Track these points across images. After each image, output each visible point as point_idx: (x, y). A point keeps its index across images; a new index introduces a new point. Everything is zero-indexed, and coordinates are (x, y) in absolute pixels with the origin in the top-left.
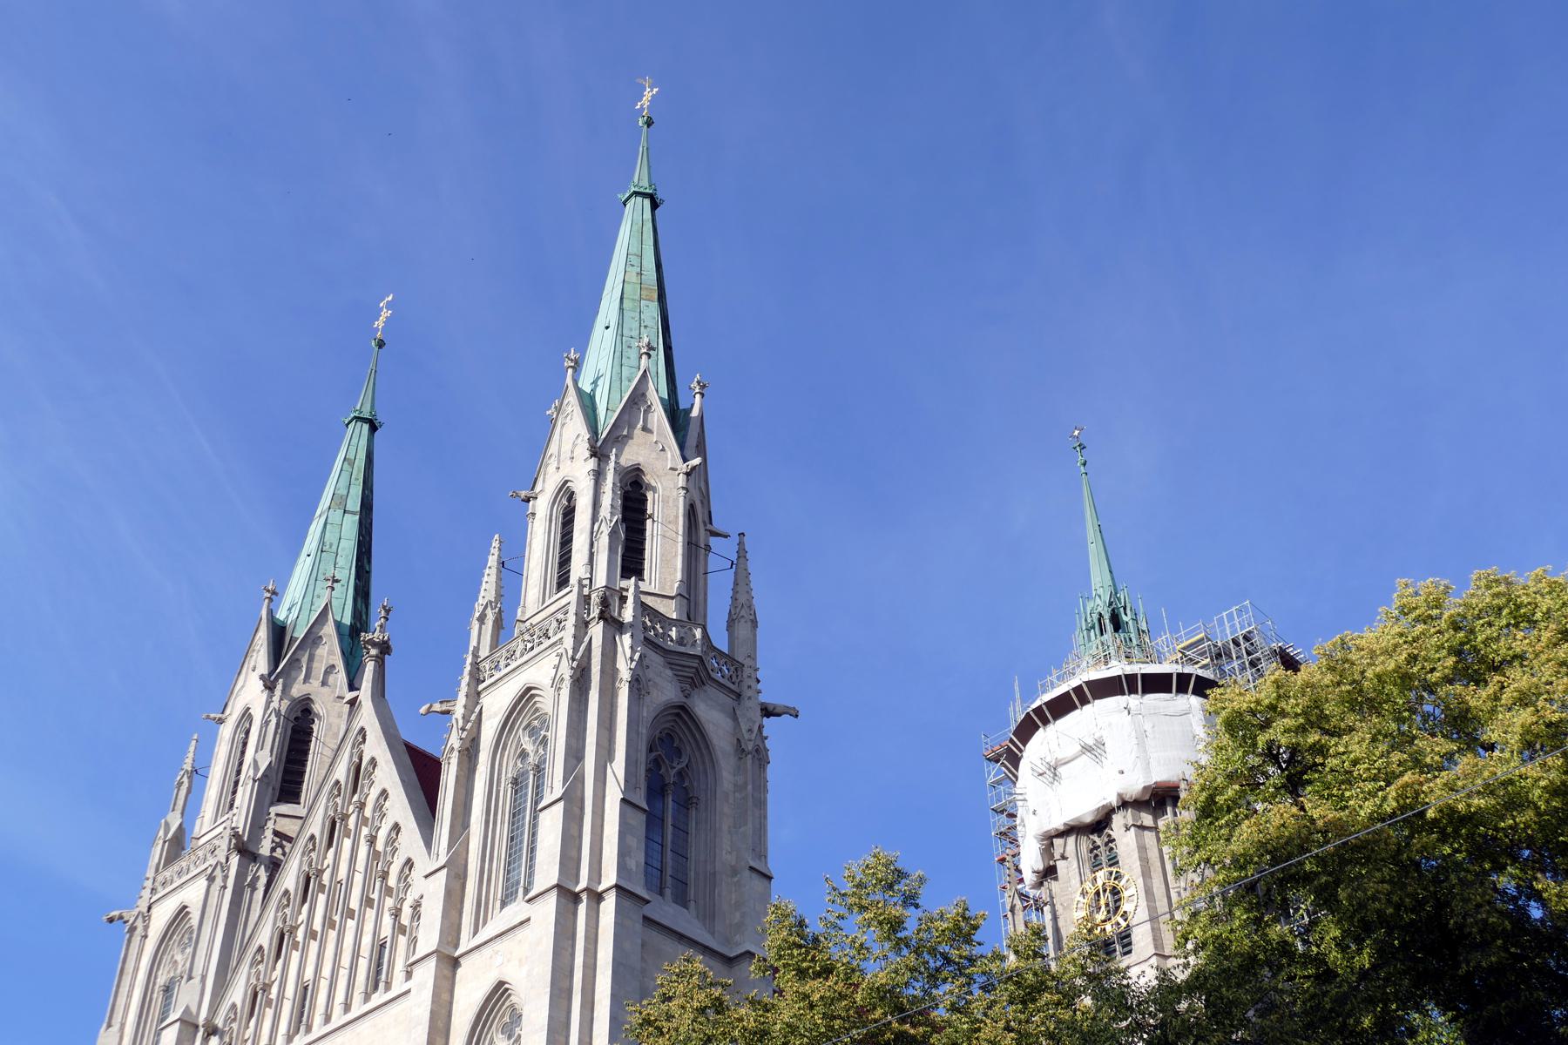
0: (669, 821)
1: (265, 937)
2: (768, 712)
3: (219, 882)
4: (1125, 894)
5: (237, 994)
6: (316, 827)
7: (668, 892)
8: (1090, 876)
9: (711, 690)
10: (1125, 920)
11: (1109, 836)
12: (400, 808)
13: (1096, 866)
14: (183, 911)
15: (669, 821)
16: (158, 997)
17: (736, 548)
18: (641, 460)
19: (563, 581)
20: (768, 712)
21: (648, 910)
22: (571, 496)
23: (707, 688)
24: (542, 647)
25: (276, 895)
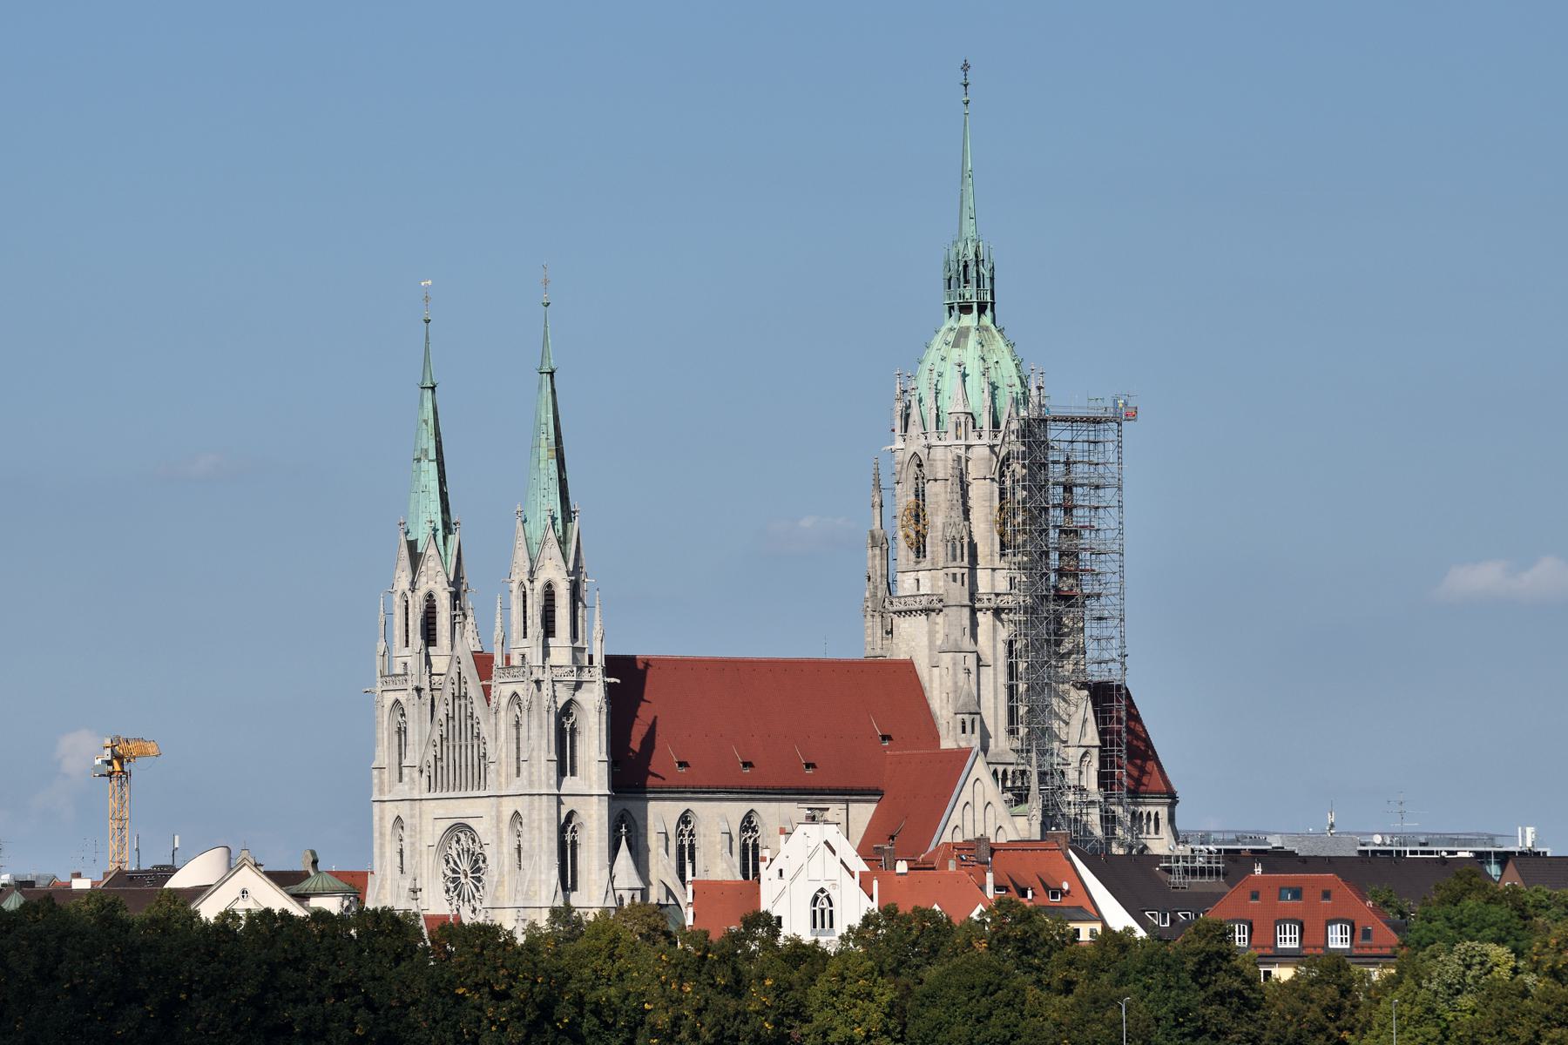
18: (550, 576)
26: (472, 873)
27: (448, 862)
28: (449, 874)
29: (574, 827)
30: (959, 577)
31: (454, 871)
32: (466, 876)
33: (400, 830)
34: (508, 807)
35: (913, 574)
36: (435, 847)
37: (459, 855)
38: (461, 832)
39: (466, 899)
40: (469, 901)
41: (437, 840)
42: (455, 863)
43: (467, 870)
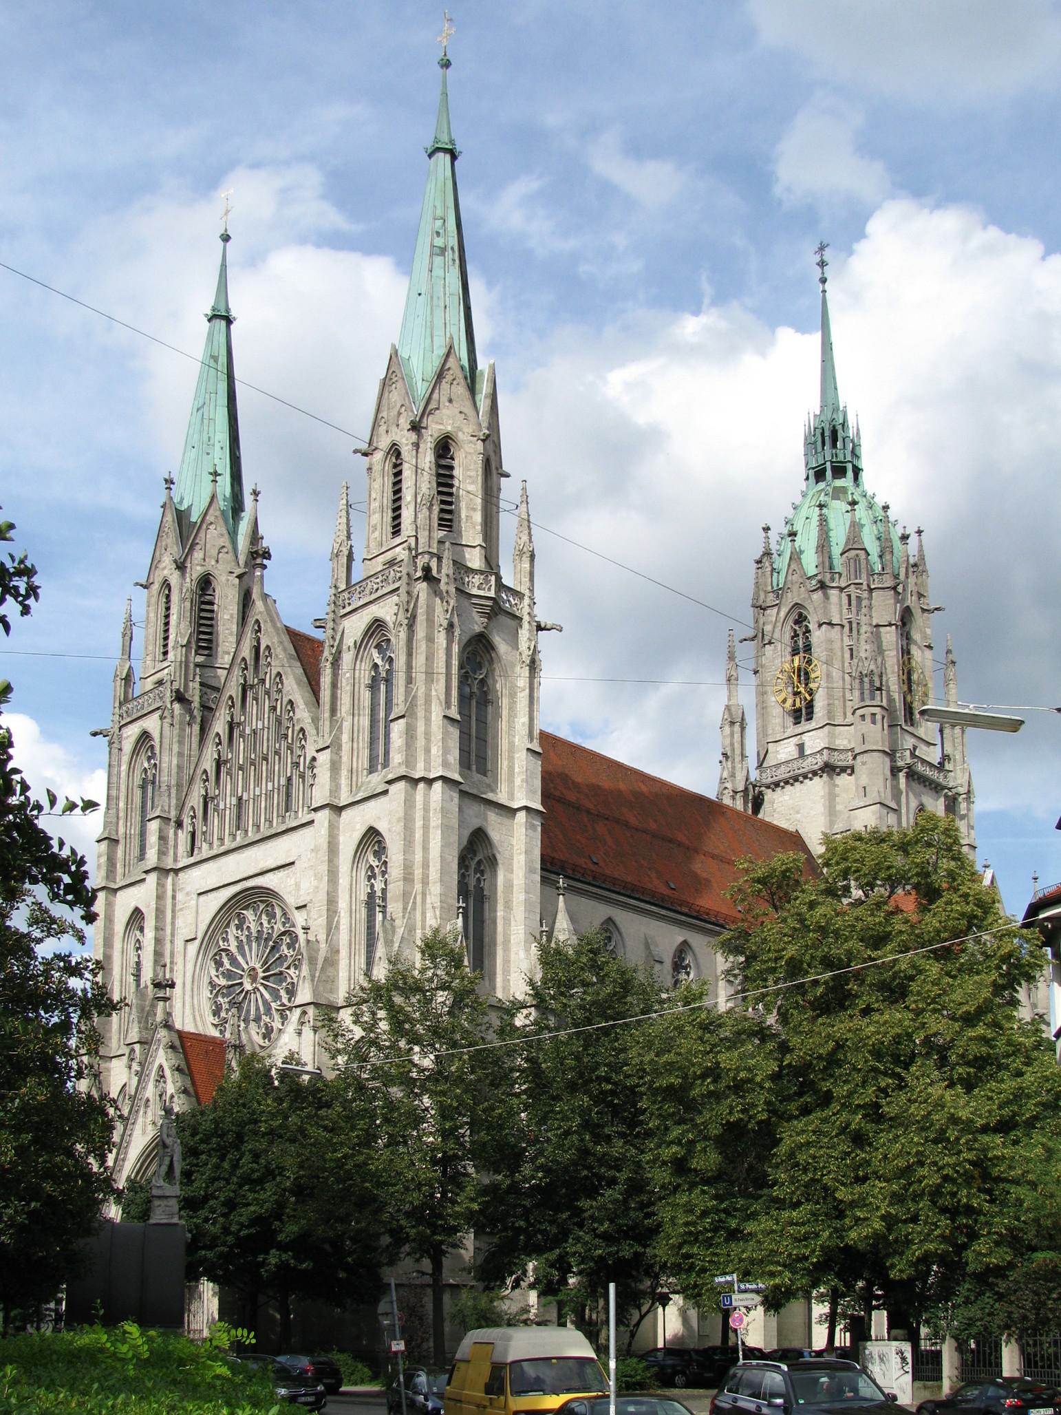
0: (474, 718)
1: (208, 764)
2: (540, 628)
3: (168, 720)
4: (813, 676)
5: (195, 800)
6: (233, 690)
7: (474, 767)
8: (789, 658)
9: (503, 619)
10: (810, 695)
11: (806, 626)
12: (293, 688)
13: (795, 652)
14: (145, 736)
15: (474, 718)
16: (138, 793)
17: (521, 492)
19: (396, 530)
20: (540, 628)
21: (462, 787)
22: (398, 454)
23: (499, 616)
24: (385, 590)
25: (212, 735)
26: (264, 972)
27: (219, 964)
28: (223, 982)
29: (479, 862)
30: (878, 717)
31: (228, 975)
32: (254, 979)
33: (138, 933)
34: (353, 825)
35: (795, 740)
36: (197, 943)
37: (240, 947)
38: (246, 908)
39: (252, 1017)
40: (258, 1019)
41: (203, 927)
42: (233, 961)
43: (258, 966)
